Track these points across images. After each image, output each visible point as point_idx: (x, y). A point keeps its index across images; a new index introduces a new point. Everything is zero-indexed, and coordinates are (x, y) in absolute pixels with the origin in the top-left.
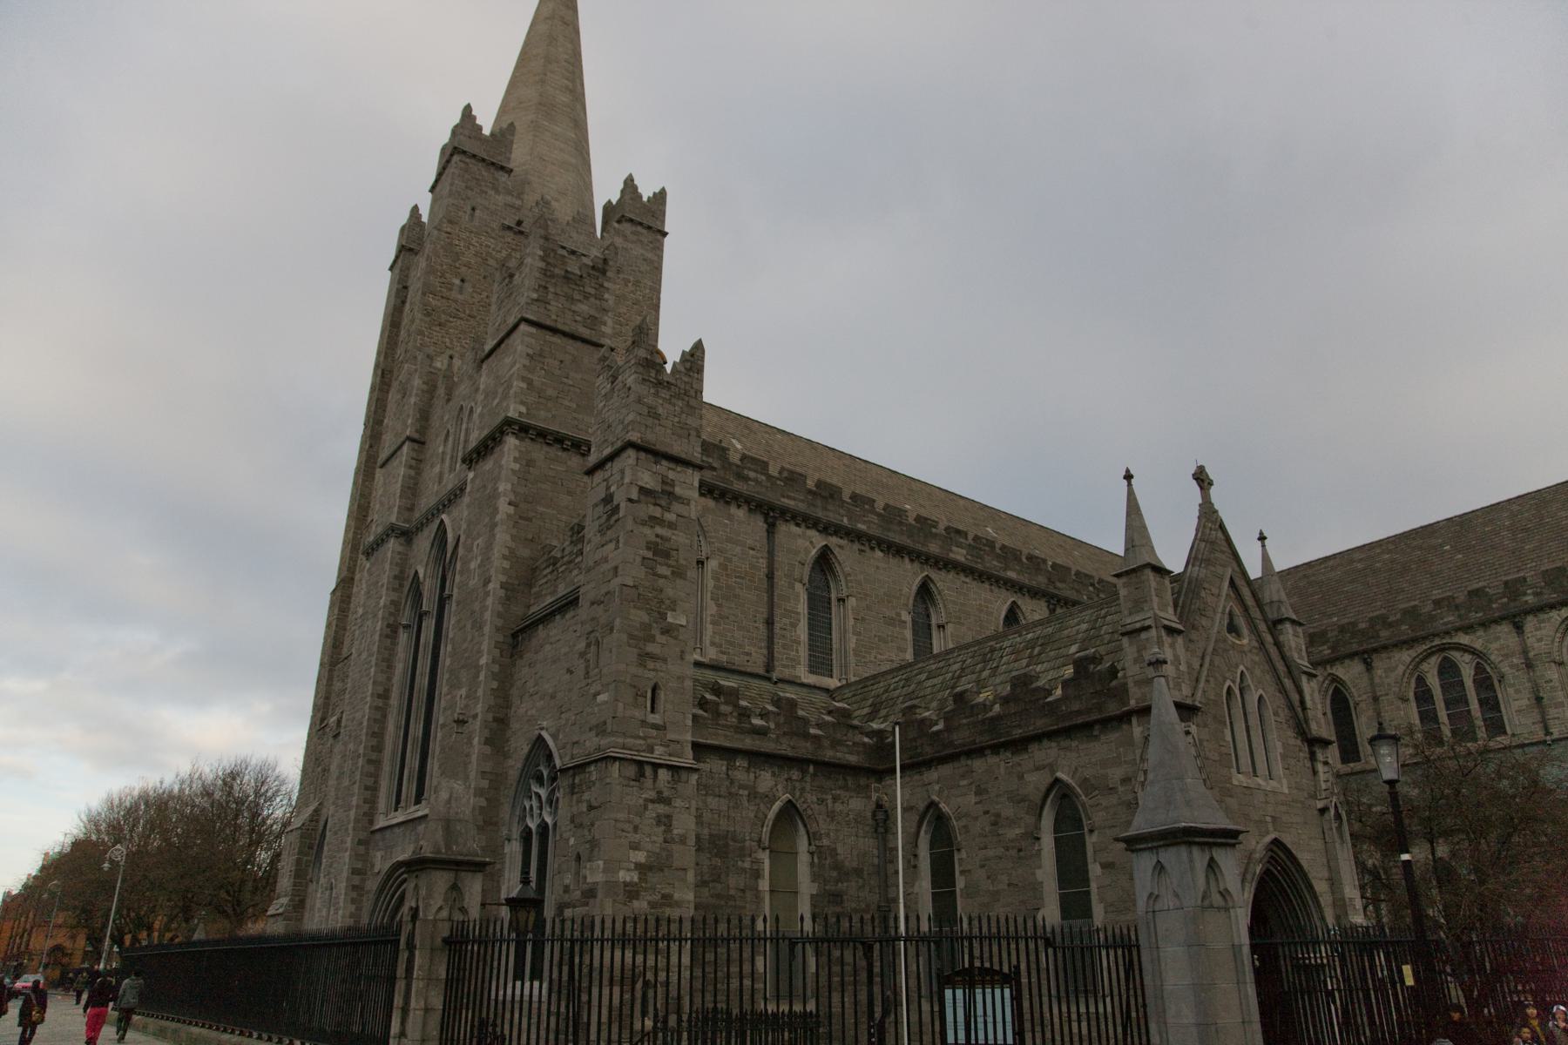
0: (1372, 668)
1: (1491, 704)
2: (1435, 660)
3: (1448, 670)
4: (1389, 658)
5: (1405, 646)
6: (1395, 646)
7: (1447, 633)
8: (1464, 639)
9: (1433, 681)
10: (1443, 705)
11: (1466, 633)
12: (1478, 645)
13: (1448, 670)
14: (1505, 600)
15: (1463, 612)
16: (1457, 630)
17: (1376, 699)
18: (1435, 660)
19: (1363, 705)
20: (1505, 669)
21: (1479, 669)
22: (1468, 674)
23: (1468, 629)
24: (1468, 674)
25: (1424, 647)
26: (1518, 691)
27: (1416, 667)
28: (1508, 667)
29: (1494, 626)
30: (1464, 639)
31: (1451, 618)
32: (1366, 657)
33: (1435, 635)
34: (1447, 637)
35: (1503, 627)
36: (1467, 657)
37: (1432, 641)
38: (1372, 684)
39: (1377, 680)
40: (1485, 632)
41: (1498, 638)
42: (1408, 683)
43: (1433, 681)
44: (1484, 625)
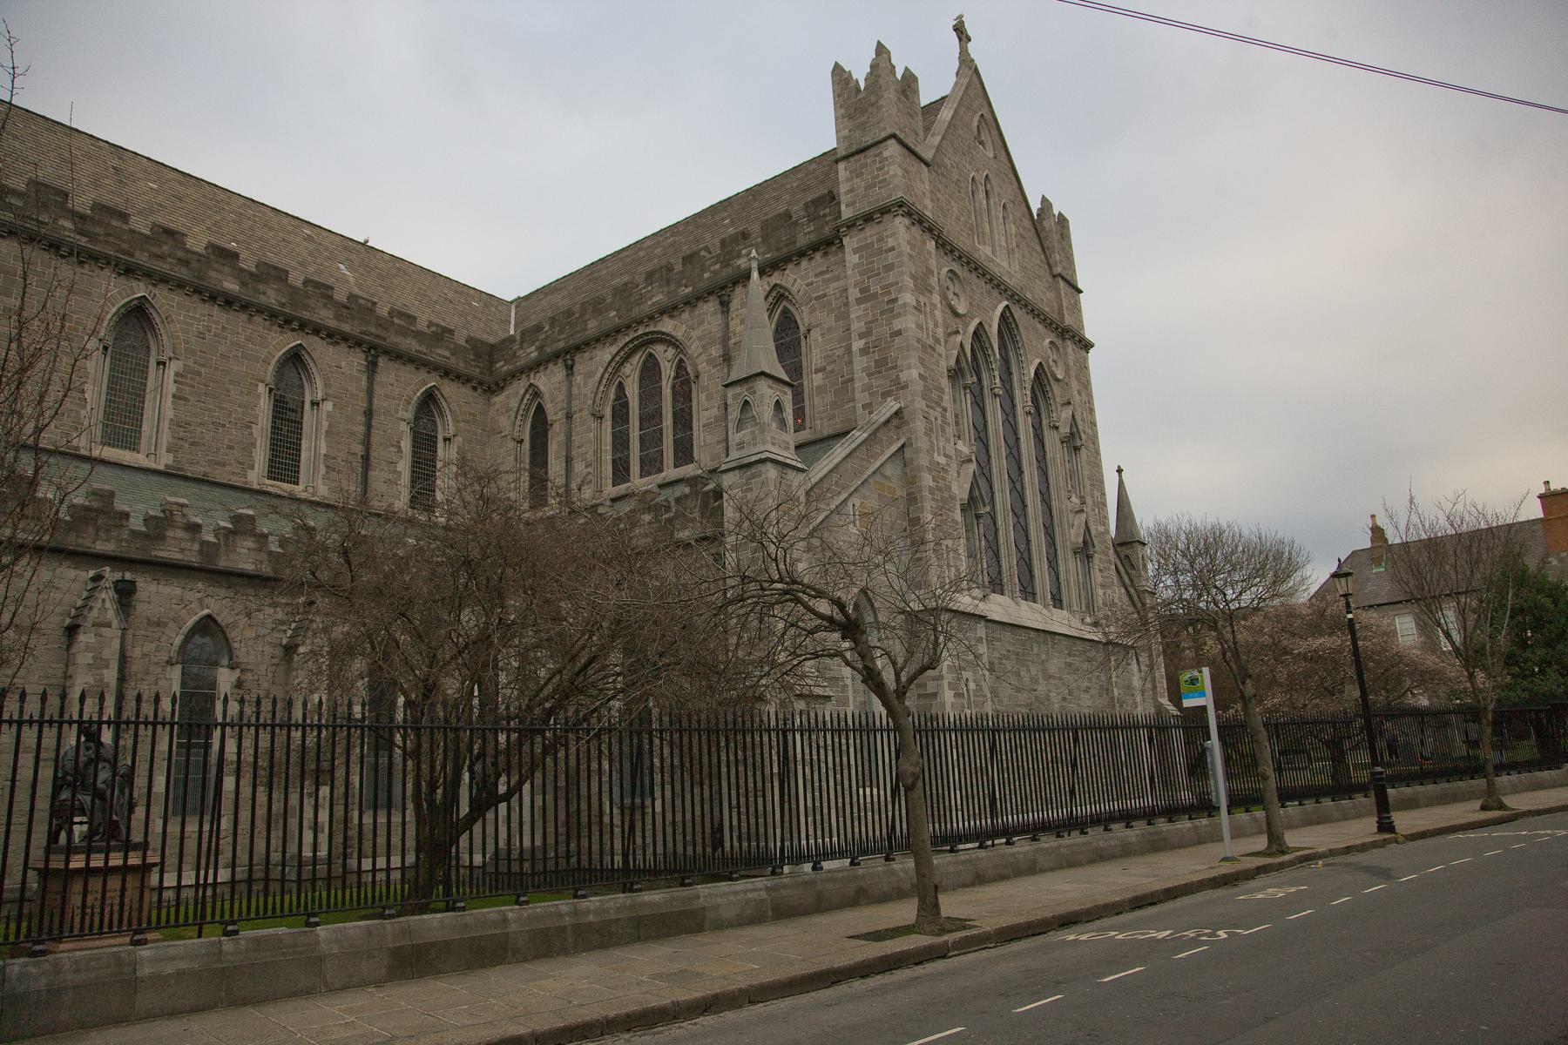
0: (572, 374)
1: (683, 420)
2: (637, 360)
3: (651, 370)
4: (591, 358)
5: (610, 340)
6: (597, 340)
7: (651, 318)
8: (667, 326)
9: (633, 391)
10: (637, 424)
11: (671, 317)
12: (679, 335)
13: (651, 370)
14: (718, 266)
15: (673, 287)
16: (662, 312)
17: (569, 416)
18: (637, 360)
19: (556, 427)
20: (703, 367)
21: (680, 366)
22: (668, 371)
23: (671, 310)
24: (668, 371)
25: (627, 340)
26: (709, 397)
27: (617, 370)
28: (703, 360)
29: (700, 304)
30: (667, 326)
31: (659, 298)
32: (567, 356)
33: (640, 322)
34: (652, 324)
35: (710, 304)
36: (671, 352)
37: (636, 331)
38: (570, 397)
39: (575, 390)
40: (691, 312)
41: (701, 323)
42: (605, 392)
43: (633, 391)
44: (691, 302)
